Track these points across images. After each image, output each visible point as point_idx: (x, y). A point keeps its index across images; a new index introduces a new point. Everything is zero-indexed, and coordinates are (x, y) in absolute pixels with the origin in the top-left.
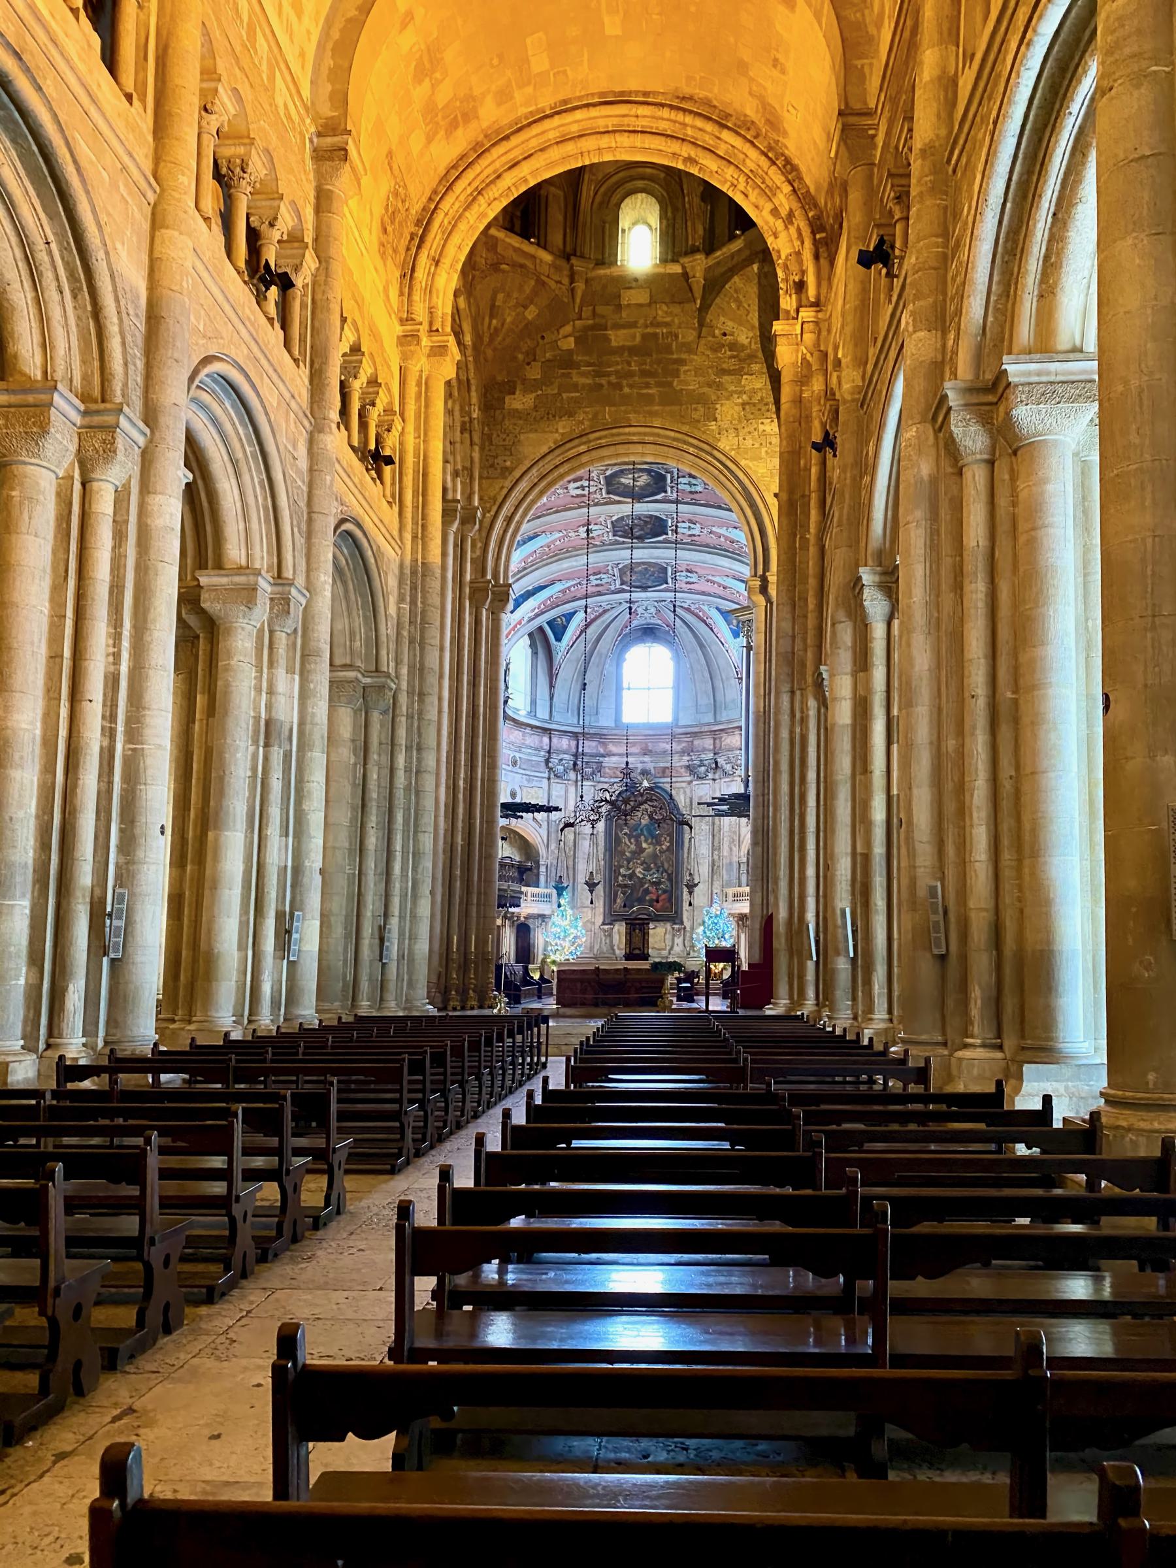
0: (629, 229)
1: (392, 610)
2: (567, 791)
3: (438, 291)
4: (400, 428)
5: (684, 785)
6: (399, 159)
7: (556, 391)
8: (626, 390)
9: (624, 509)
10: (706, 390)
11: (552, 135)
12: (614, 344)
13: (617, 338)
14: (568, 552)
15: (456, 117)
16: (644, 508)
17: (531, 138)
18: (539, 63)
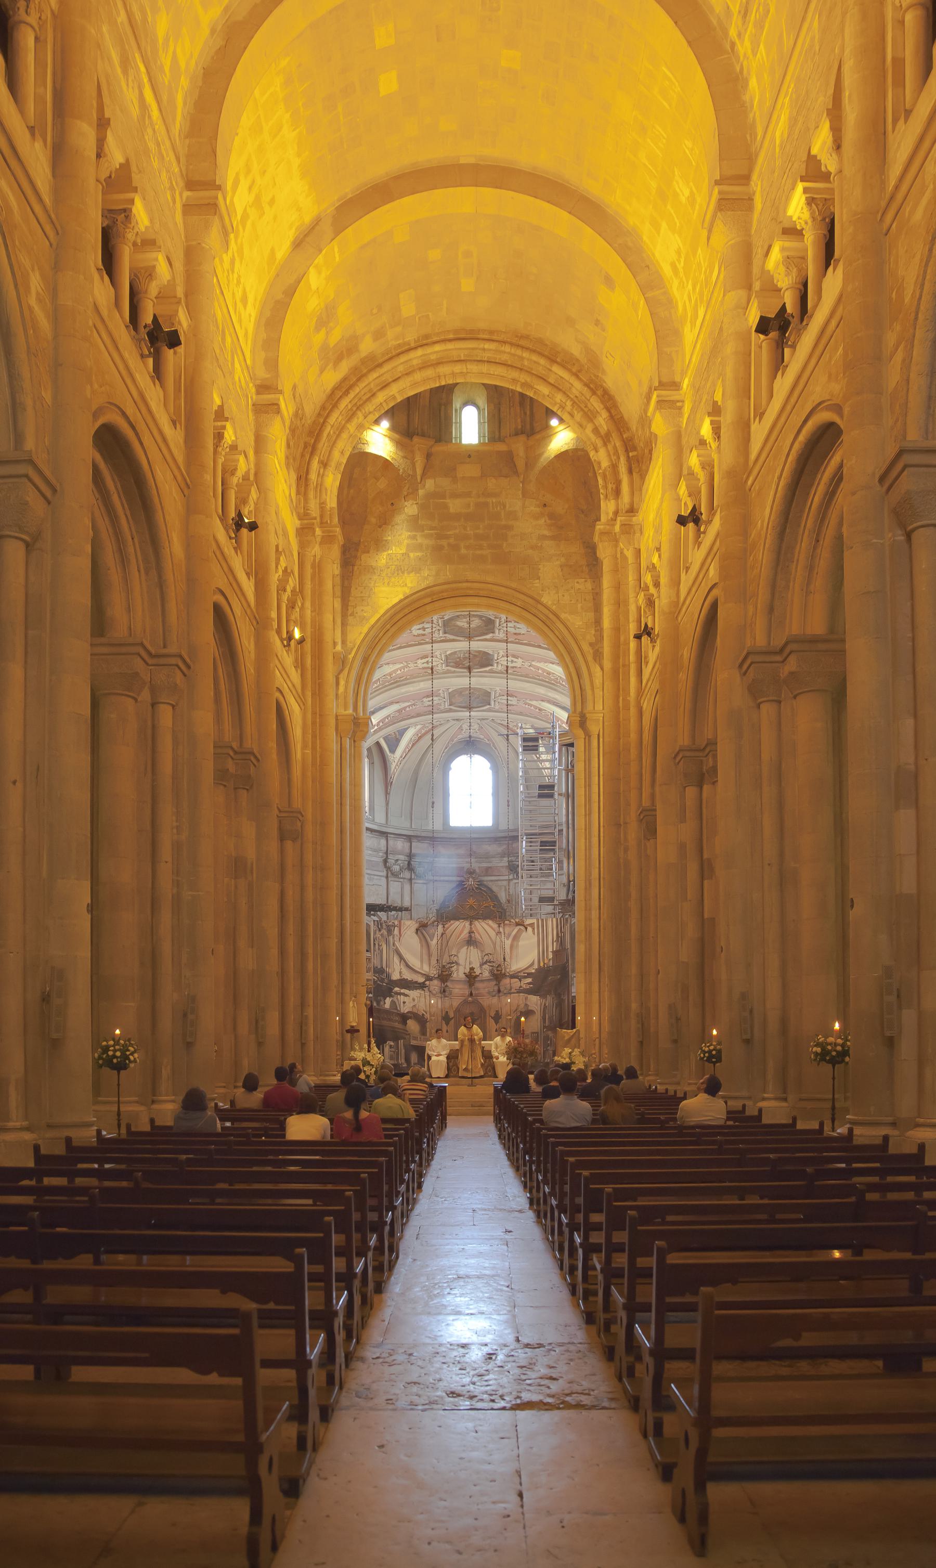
0: (461, 409)
1: (299, 756)
2: (402, 888)
3: (326, 489)
4: (300, 605)
5: (505, 883)
6: (300, 389)
7: (404, 551)
8: (463, 551)
9: (461, 646)
10: (530, 552)
11: (415, 362)
12: (452, 510)
13: (455, 506)
14: (406, 679)
15: (342, 352)
16: (477, 645)
17: (399, 365)
18: (408, 309)
